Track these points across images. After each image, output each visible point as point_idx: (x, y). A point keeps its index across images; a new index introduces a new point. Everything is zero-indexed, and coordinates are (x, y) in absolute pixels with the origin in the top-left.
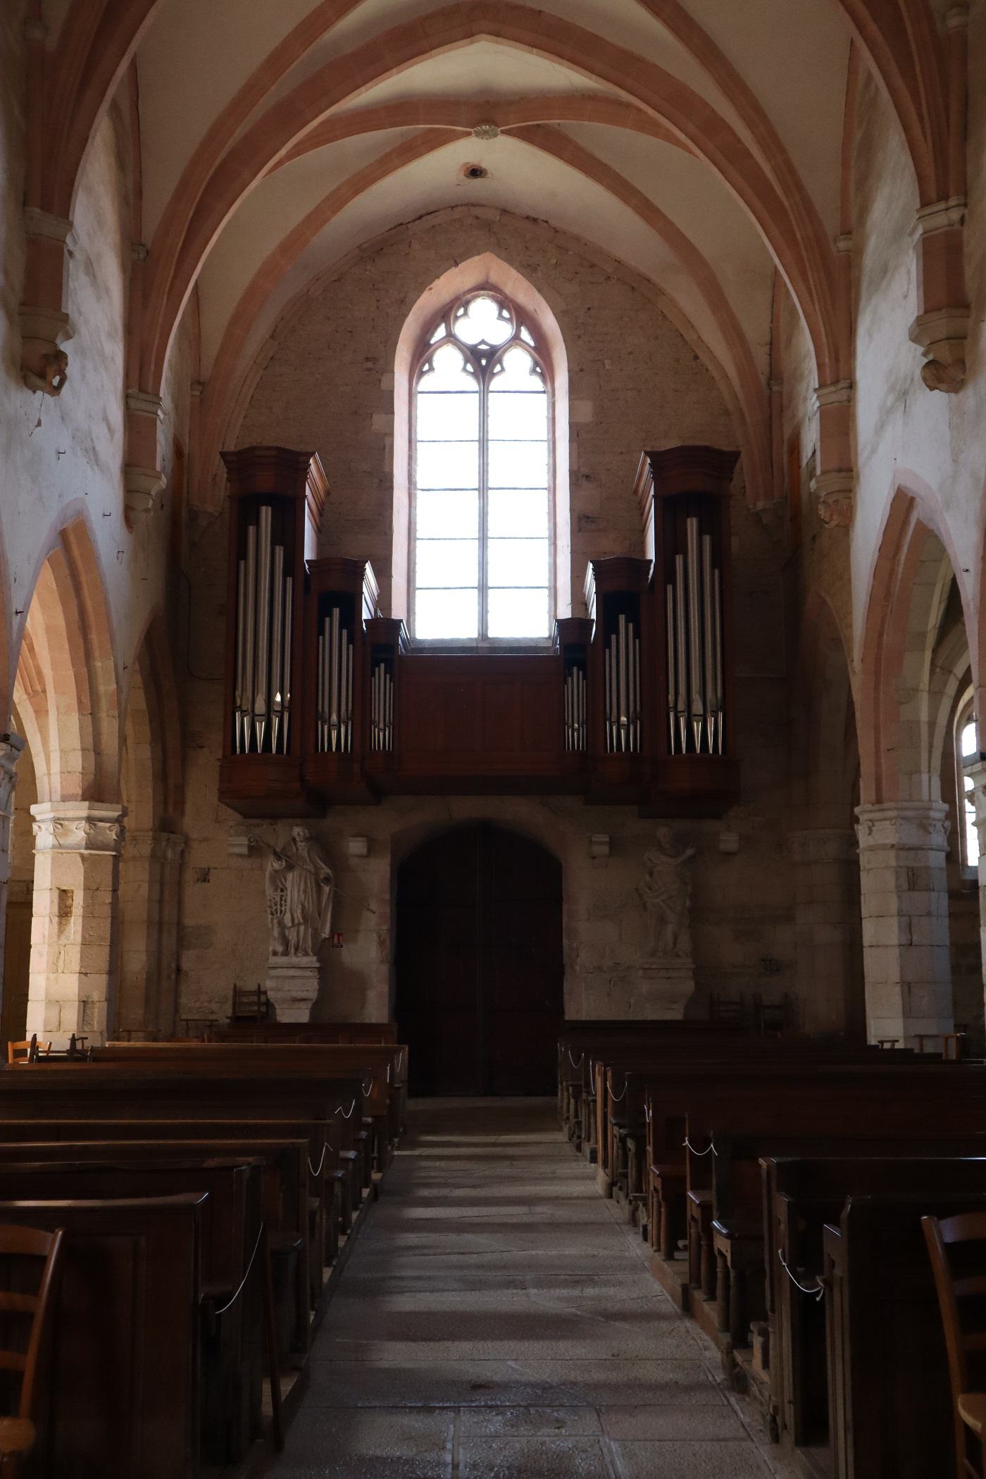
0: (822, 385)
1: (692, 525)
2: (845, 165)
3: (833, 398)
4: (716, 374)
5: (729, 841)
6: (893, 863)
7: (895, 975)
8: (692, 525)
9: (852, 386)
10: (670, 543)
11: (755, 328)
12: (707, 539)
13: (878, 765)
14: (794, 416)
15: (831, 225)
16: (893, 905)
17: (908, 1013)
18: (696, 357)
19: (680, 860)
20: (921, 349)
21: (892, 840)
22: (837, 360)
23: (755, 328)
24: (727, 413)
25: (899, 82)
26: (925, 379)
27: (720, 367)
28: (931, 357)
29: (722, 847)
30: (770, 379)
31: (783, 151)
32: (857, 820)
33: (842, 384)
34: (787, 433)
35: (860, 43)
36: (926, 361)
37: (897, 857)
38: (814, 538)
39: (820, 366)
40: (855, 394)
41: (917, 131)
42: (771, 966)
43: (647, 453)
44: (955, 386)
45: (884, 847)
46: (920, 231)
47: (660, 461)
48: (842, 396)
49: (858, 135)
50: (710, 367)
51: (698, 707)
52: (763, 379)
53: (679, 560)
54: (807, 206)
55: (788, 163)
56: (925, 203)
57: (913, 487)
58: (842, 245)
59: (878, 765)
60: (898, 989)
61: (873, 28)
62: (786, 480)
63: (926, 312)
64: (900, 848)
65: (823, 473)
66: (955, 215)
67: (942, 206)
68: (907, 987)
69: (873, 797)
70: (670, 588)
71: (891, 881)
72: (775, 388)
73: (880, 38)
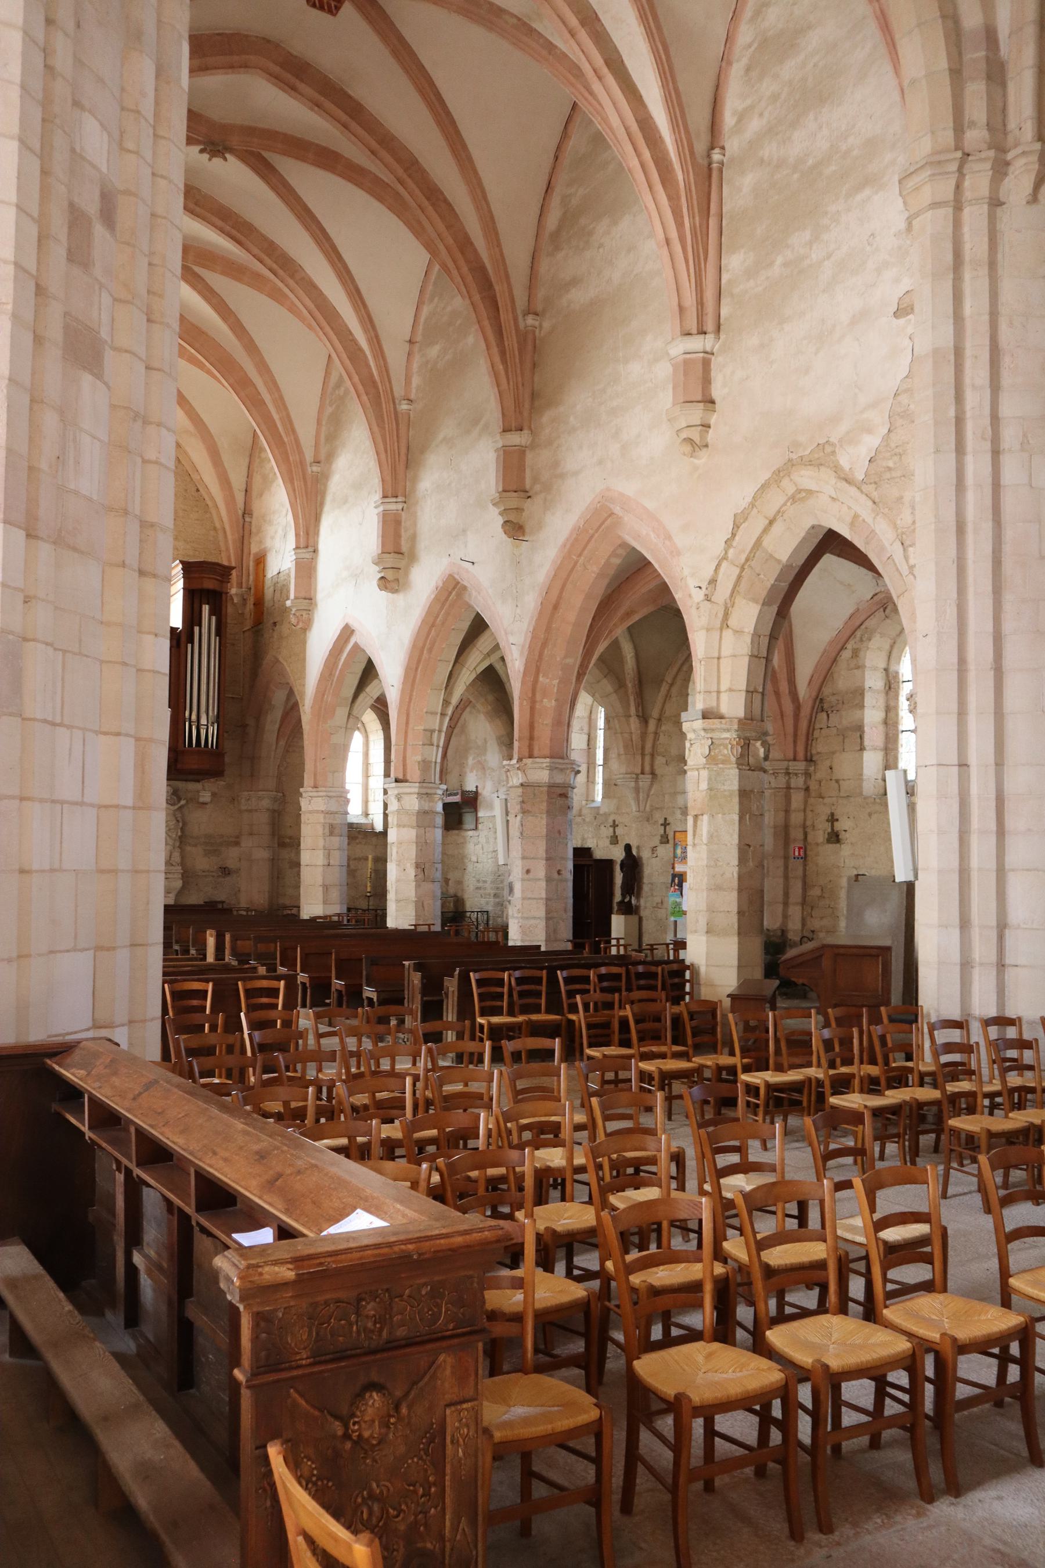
0: (297, 548)
1: (206, 608)
2: (319, 422)
3: (303, 556)
4: (209, 503)
5: (206, 797)
6: (322, 821)
7: (319, 880)
8: (206, 608)
9: (315, 551)
10: (191, 616)
11: (238, 481)
12: (214, 618)
13: (316, 767)
14: (261, 542)
15: (309, 456)
16: (321, 843)
17: (325, 902)
18: (198, 490)
19: (176, 807)
20: (377, 568)
21: (323, 808)
22: (308, 534)
23: (238, 481)
24: (215, 529)
25: (376, 429)
26: (379, 586)
27: (212, 499)
28: (382, 575)
29: (201, 800)
30: (244, 513)
31: (286, 408)
32: (301, 795)
33: (311, 549)
34: (254, 549)
35: (334, 355)
36: (380, 575)
37: (325, 818)
38: (275, 624)
39: (297, 535)
40: (317, 556)
41: (383, 456)
42: (225, 871)
43: (182, 562)
44: (395, 591)
45: (317, 812)
46: (381, 509)
47: (189, 568)
48: (307, 556)
49: (329, 410)
50: (207, 498)
51: (203, 721)
52: (240, 513)
53: (196, 629)
54: (297, 441)
55: (289, 416)
56: (384, 497)
57: (354, 625)
58: (315, 469)
59: (316, 767)
60: (321, 889)
61: (365, 398)
62: (251, 578)
63: (383, 553)
64: (327, 813)
65: (296, 598)
66: (400, 506)
67: (394, 500)
68: (326, 888)
69: (312, 784)
70: (189, 646)
71: (320, 830)
72: (247, 519)
73: (368, 405)
